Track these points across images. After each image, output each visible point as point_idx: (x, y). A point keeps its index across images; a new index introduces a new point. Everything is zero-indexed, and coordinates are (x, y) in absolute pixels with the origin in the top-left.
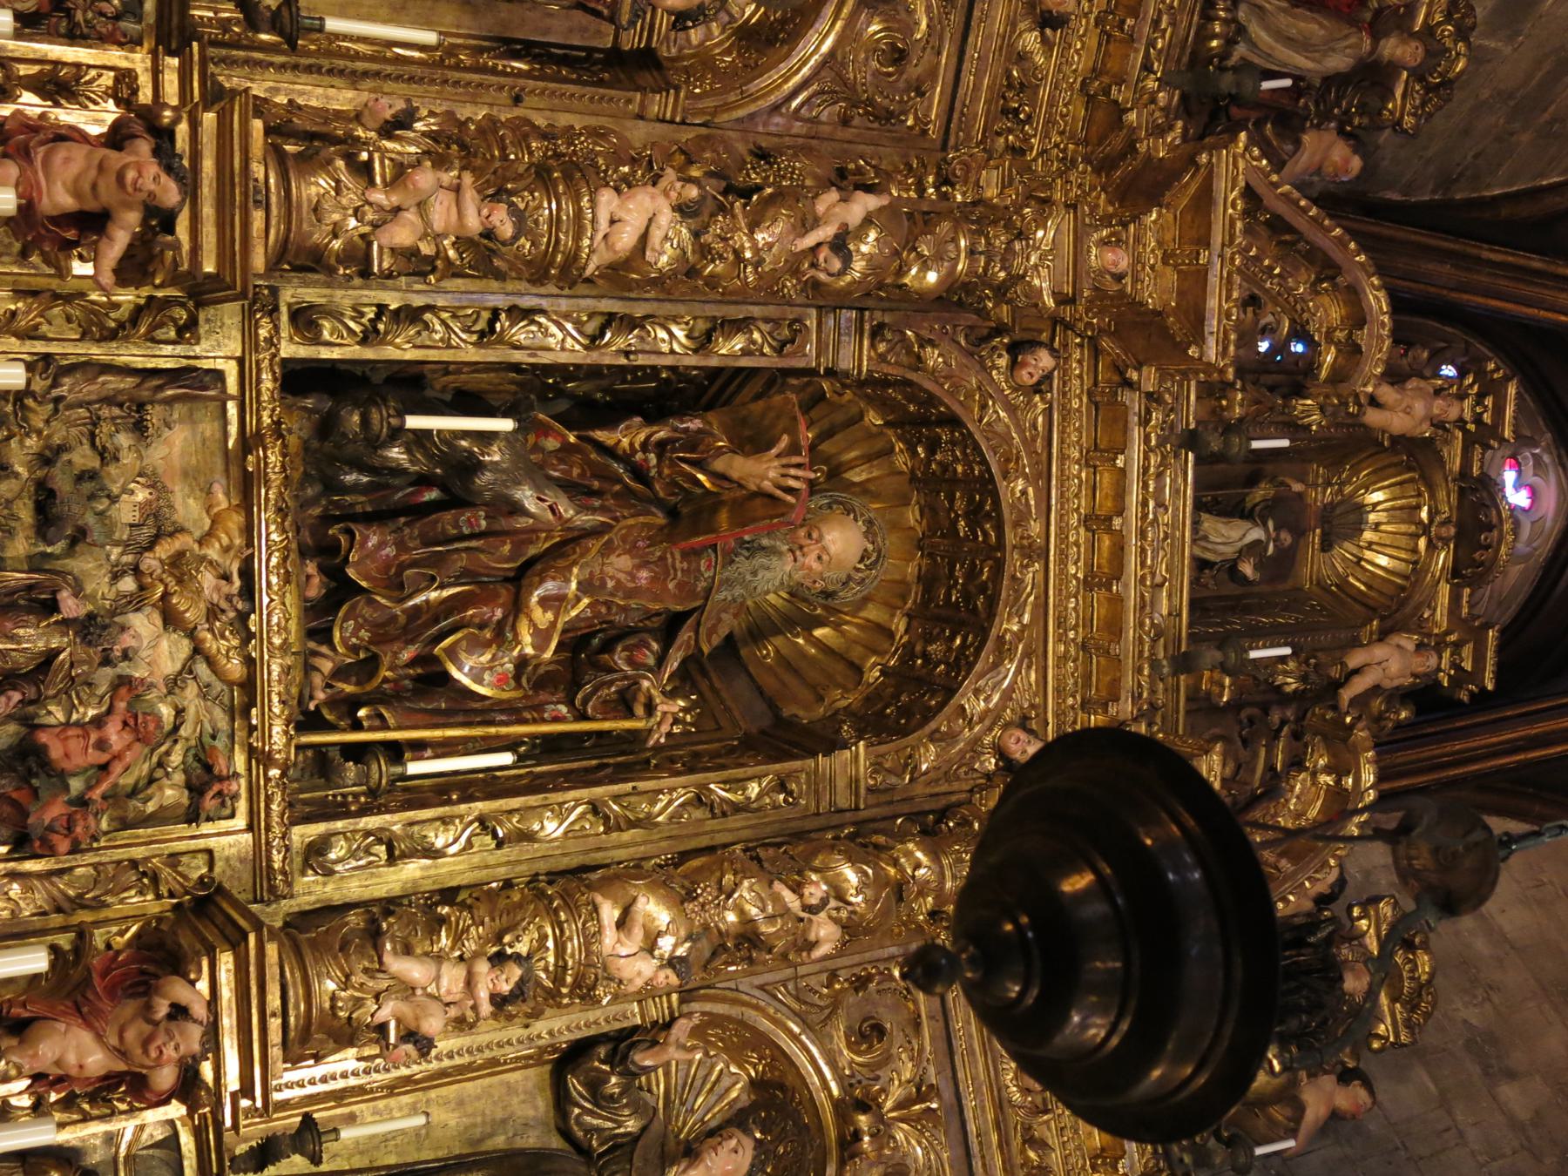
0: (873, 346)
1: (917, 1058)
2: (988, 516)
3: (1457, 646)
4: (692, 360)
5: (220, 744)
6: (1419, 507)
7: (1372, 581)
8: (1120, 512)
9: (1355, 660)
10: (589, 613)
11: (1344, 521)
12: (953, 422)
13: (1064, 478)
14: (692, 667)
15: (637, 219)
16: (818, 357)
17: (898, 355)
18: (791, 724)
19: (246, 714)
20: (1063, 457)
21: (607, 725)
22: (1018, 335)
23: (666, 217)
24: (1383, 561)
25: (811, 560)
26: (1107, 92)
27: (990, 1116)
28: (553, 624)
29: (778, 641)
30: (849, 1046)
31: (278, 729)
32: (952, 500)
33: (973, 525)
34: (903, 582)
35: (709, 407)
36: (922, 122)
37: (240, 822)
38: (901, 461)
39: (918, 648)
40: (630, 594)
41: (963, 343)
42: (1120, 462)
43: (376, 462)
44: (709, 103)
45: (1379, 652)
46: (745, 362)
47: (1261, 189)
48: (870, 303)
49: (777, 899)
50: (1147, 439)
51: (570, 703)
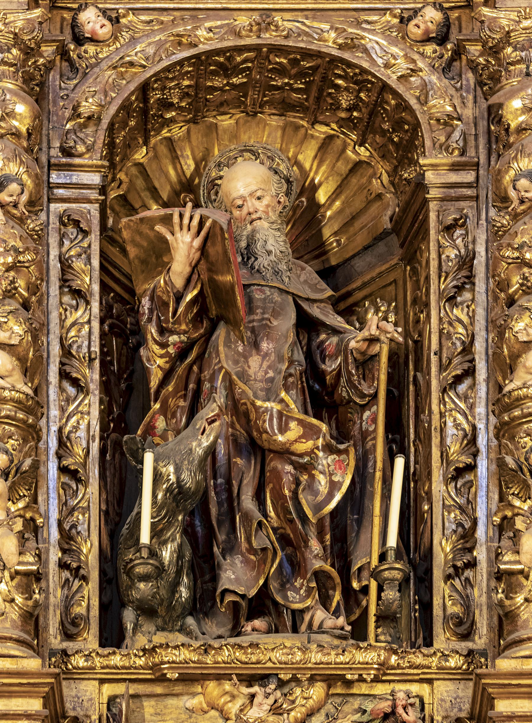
0: (80, 156)
5: (369, 706)
10: (294, 392)
12: (144, 88)
14: (342, 306)
16: (89, 201)
17: (87, 135)
19: (349, 684)
21: (383, 377)
22: (67, 36)
28: (301, 422)
31: (360, 657)
32: (213, 89)
34: (284, 129)
35: (132, 292)
40: (280, 359)
41: (75, 82)
43: (172, 570)
48: (44, 159)
51: (364, 408)
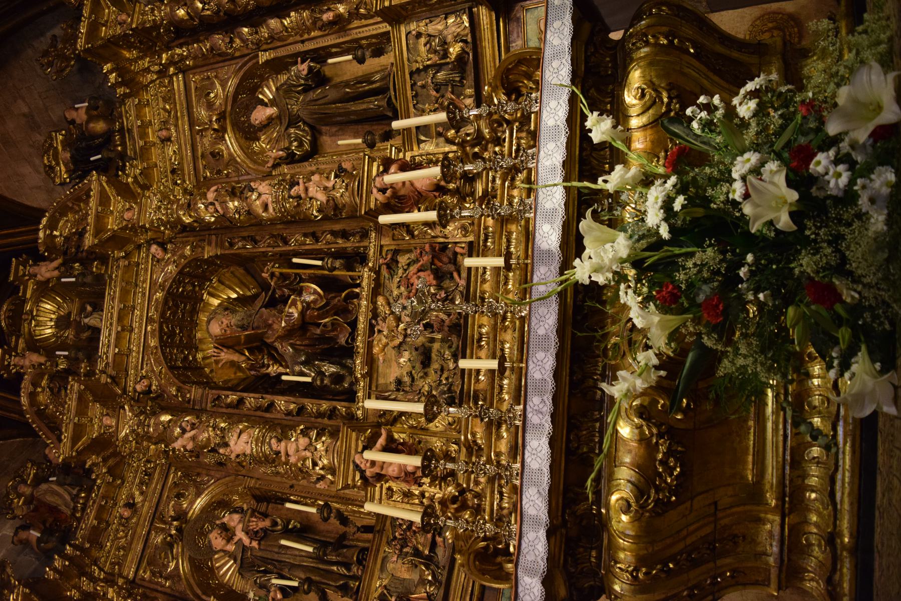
1: (203, 145)
2: (166, 334)
3: (24, 275)
4: (245, 395)
6: (35, 326)
7: (54, 300)
8: (118, 333)
9: (56, 273)
11: (62, 323)
12: (172, 368)
13: (138, 346)
15: (242, 443)
18: (240, 265)
20: (138, 353)
23: (232, 443)
24: (48, 307)
25: (225, 322)
26: (114, 480)
27: (180, 122)
29: (249, 294)
30: (222, 151)
33: (174, 331)
36: (175, 473)
37: (385, 249)
38: (199, 356)
39: (197, 289)
42: (117, 350)
44: (237, 483)
45: (48, 275)
46: (230, 393)
47: (56, 441)
49: (222, 208)
50: (107, 357)
